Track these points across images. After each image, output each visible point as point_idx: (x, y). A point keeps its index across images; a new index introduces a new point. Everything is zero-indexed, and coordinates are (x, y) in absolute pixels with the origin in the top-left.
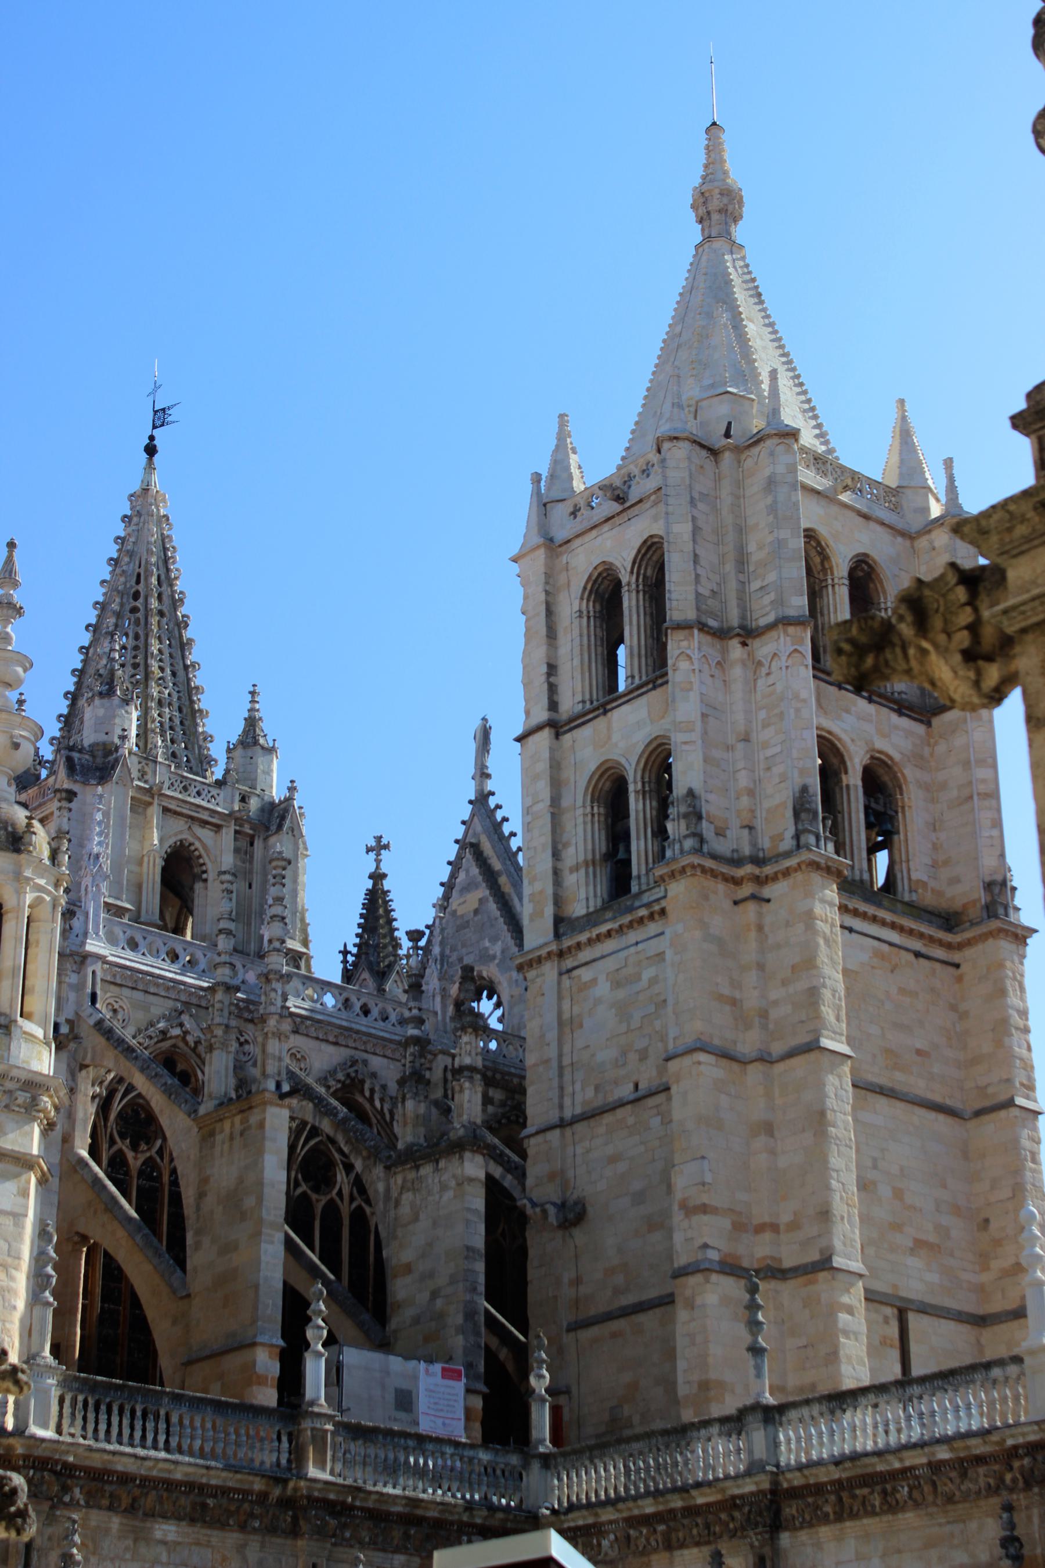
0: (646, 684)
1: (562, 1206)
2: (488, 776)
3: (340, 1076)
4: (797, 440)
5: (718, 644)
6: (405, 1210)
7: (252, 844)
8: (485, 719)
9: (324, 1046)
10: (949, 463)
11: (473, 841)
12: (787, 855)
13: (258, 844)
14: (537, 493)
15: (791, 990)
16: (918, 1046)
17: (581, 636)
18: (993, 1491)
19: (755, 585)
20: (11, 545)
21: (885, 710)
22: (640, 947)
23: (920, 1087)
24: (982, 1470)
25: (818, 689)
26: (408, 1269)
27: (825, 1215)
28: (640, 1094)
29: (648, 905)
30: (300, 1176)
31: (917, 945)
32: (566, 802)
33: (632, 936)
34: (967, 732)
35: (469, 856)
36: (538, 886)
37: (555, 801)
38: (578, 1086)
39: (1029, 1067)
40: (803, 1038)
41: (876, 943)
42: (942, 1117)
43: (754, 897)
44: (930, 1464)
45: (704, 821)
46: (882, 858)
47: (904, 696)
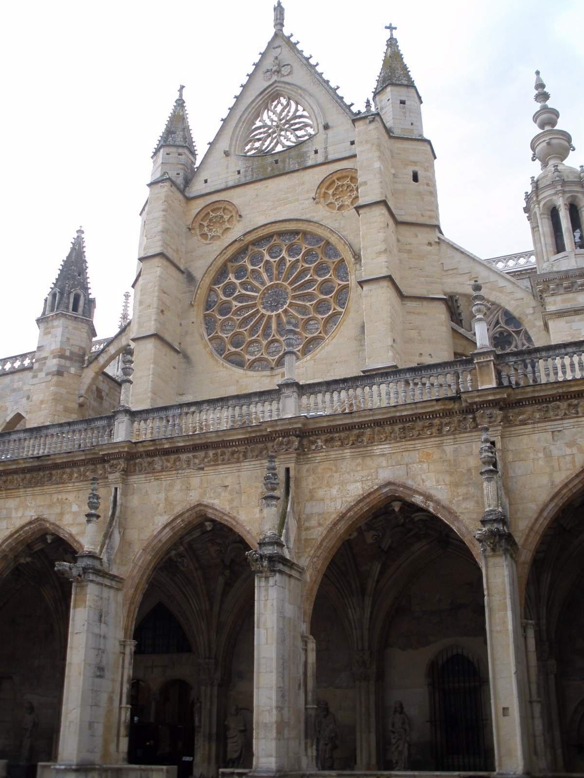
20: (538, 73)
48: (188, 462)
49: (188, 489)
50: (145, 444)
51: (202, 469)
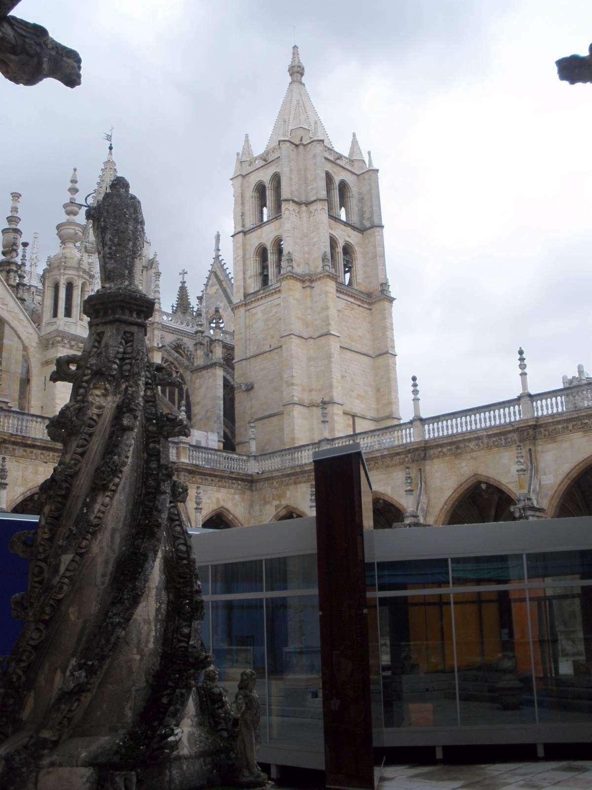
0: (274, 219)
1: (246, 385)
2: (219, 250)
3: (174, 343)
4: (323, 143)
6: (197, 385)
7: (142, 272)
8: (218, 232)
10: (369, 153)
11: (215, 270)
12: (321, 273)
13: (144, 272)
14: (238, 159)
15: (321, 315)
17: (252, 203)
18: (402, 463)
19: (310, 188)
20: (75, 170)
21: (349, 228)
22: (272, 302)
24: (398, 457)
25: (329, 222)
26: (198, 403)
27: (331, 386)
28: (272, 348)
29: (274, 289)
31: (359, 303)
32: (247, 256)
33: (269, 299)
34: (375, 236)
35: (213, 276)
36: (238, 283)
37: (244, 257)
38: (251, 346)
39: (393, 340)
40: (324, 331)
42: (366, 357)
43: (309, 286)
44: (381, 456)
45: (294, 262)
46: (348, 275)
48: (36, 455)
49: (36, 473)
50: (17, 437)
51: (46, 463)
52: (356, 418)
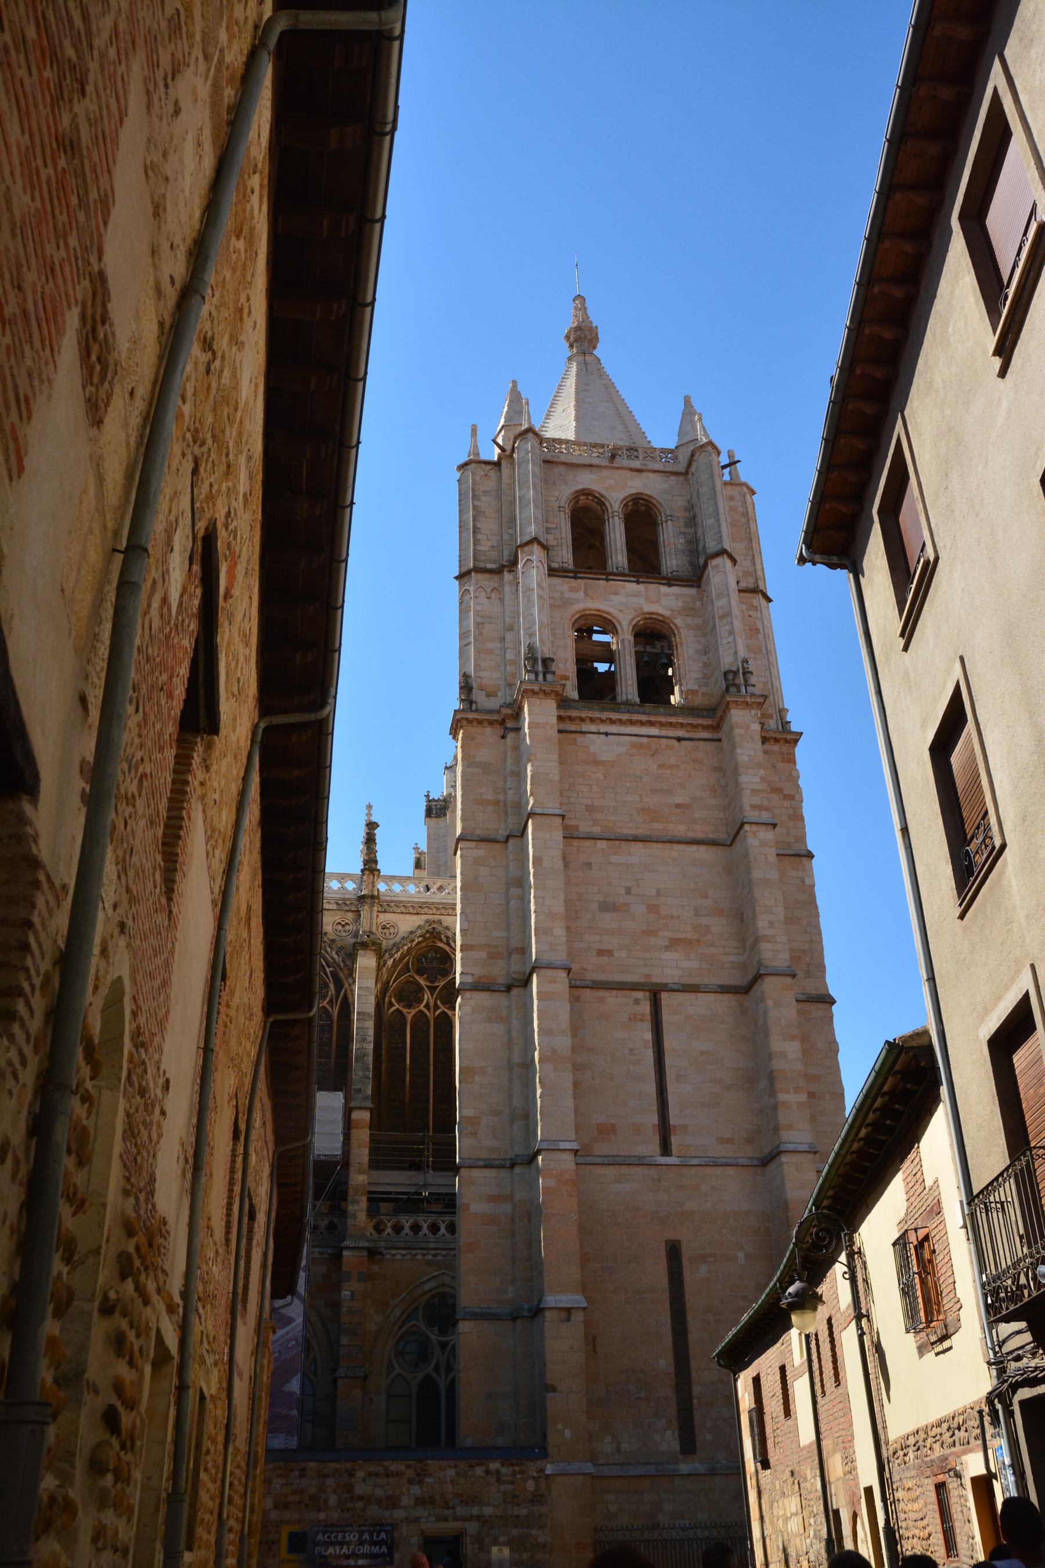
5: (496, 578)
9: (408, 917)
16: (678, 802)
23: (680, 830)
30: (393, 1000)
31: (681, 733)
41: (634, 738)
47: (674, 573)
52: (664, 996)
